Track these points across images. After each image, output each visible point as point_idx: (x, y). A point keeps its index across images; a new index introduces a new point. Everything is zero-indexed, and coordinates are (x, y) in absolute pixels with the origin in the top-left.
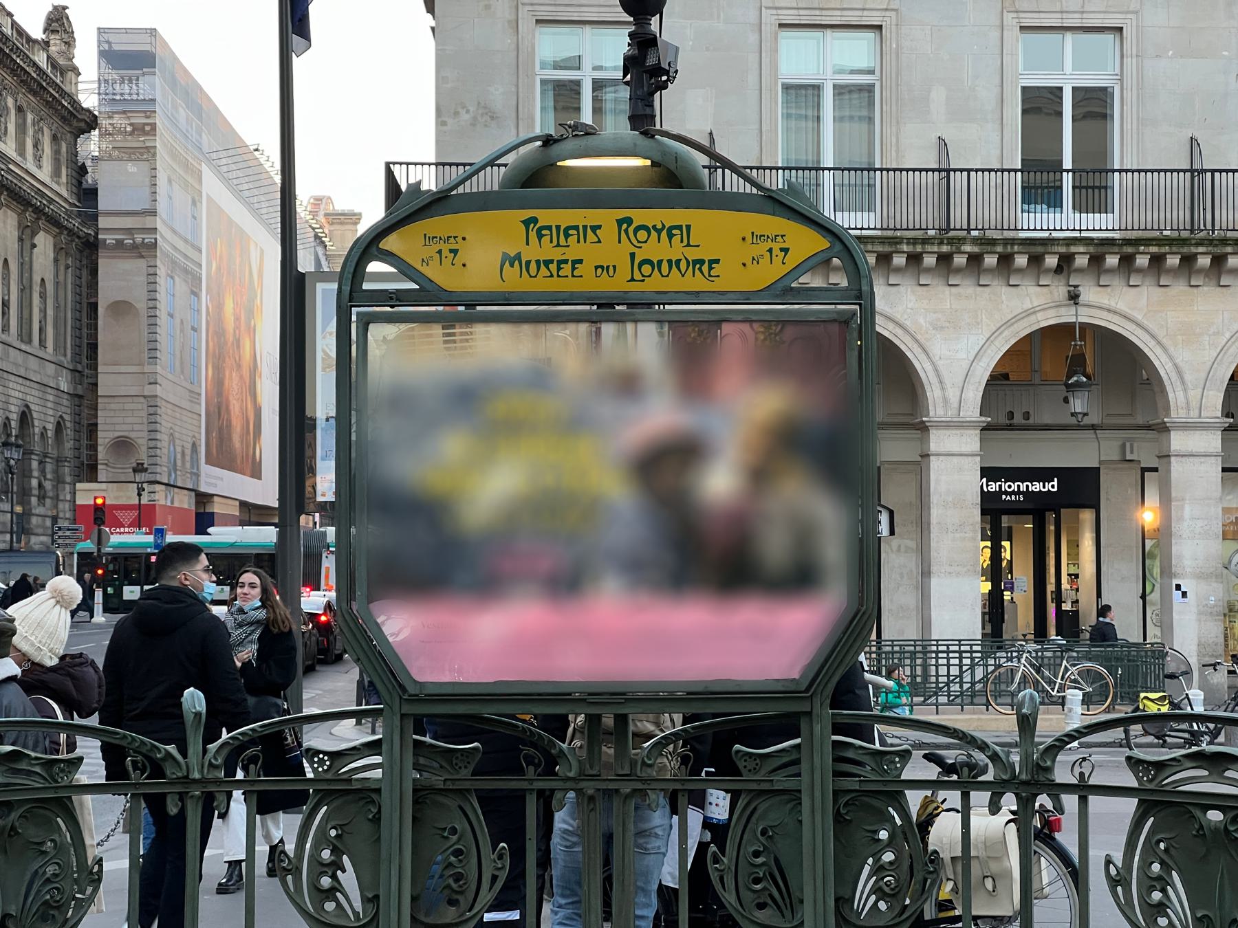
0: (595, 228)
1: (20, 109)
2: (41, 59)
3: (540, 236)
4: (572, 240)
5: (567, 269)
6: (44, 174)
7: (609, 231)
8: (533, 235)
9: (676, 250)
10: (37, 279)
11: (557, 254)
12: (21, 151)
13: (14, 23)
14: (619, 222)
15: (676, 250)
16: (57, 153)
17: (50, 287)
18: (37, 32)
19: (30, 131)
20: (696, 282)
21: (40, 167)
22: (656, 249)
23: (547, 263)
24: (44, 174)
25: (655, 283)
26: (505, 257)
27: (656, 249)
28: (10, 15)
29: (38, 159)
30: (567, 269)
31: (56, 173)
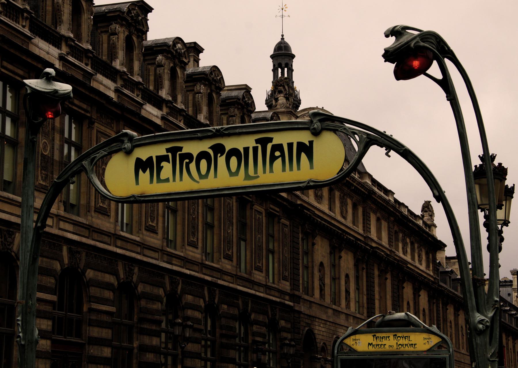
0: (388, 337)
1: (412, 244)
2: (420, 223)
3: (376, 339)
4: (384, 340)
5: (383, 346)
6: (423, 267)
7: (392, 337)
8: (375, 339)
9: (406, 342)
10: (421, 309)
11: (380, 343)
12: (413, 258)
13: (409, 211)
14: (394, 336)
15: (406, 342)
16: (428, 258)
17: (427, 311)
18: (418, 212)
19: (417, 251)
20: (411, 349)
21: (421, 264)
22: (402, 341)
23: (378, 345)
24: (423, 267)
25: (402, 349)
26: (369, 344)
27: (402, 341)
28: (407, 207)
29: (420, 261)
30: (383, 346)
31: (428, 267)
